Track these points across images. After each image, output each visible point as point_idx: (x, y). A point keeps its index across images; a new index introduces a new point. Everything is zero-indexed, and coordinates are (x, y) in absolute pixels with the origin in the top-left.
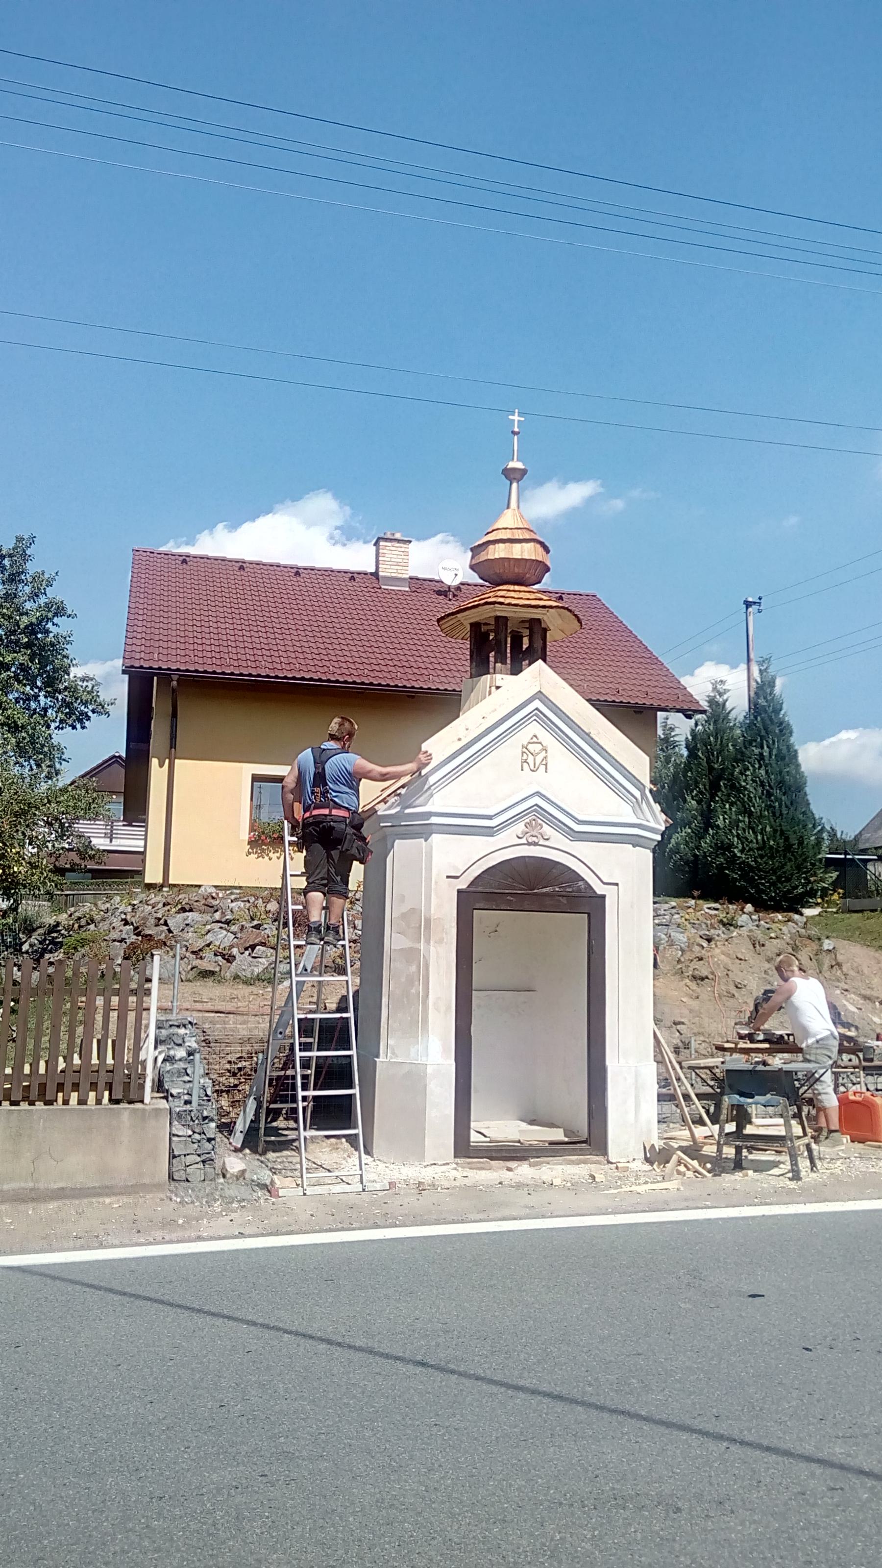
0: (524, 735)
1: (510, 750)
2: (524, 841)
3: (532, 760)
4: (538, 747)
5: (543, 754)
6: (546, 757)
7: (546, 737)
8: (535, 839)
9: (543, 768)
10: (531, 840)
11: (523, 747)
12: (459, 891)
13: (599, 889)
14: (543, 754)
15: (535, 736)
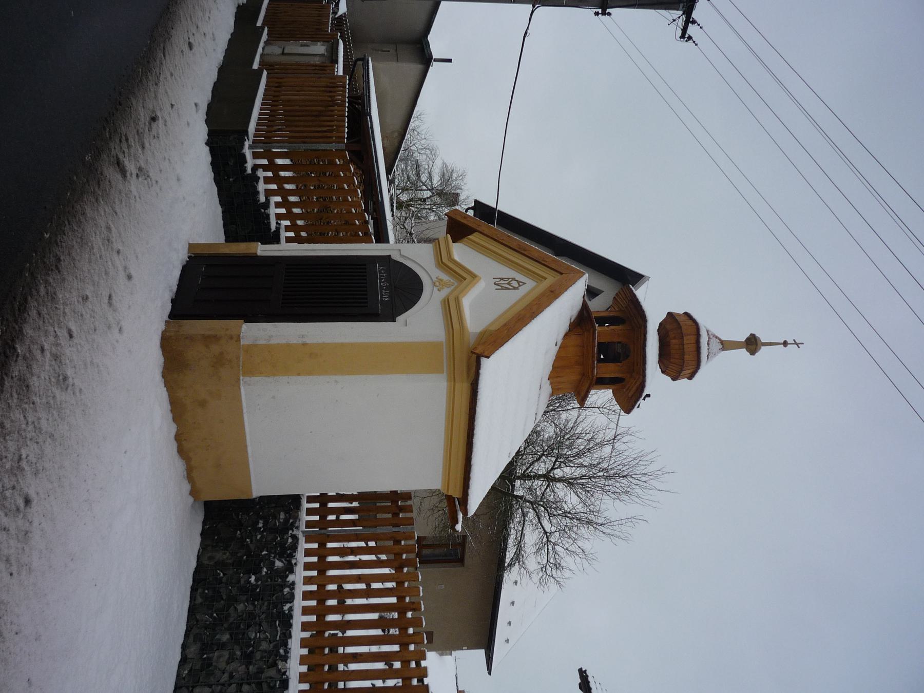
2: (435, 279)
12: (390, 256)
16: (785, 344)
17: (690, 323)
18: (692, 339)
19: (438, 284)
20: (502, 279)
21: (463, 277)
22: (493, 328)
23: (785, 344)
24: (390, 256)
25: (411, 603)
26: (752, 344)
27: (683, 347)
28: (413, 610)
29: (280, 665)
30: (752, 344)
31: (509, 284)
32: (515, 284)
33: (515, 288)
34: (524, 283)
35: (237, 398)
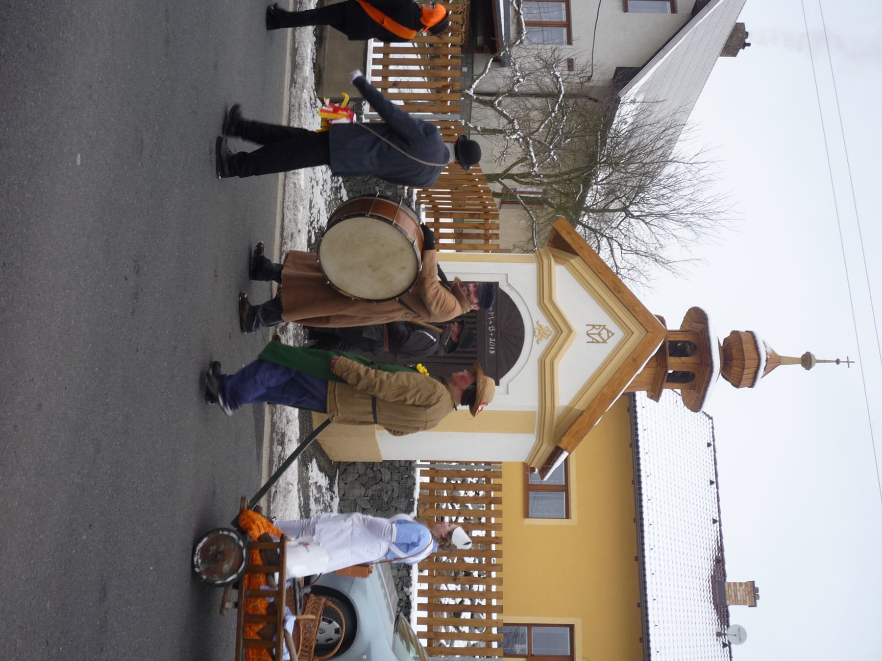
0: (612, 326)
1: (602, 317)
2: (535, 325)
3: (596, 334)
4: (605, 337)
5: (601, 340)
6: (598, 342)
7: (613, 343)
8: (537, 333)
9: (591, 340)
10: (537, 331)
11: (604, 326)
12: (497, 283)
13: (502, 381)
14: (601, 340)
15: (613, 334)
16: (838, 362)
17: (754, 355)
18: (753, 370)
19: (539, 333)
20: (594, 326)
21: (560, 330)
22: (579, 407)
23: (838, 362)
24: (497, 283)
25: (496, 538)
26: (807, 361)
27: (743, 360)
28: (496, 543)
29: (405, 589)
30: (807, 361)
31: (599, 334)
32: (604, 334)
33: (604, 342)
34: (613, 334)
35: (376, 445)
